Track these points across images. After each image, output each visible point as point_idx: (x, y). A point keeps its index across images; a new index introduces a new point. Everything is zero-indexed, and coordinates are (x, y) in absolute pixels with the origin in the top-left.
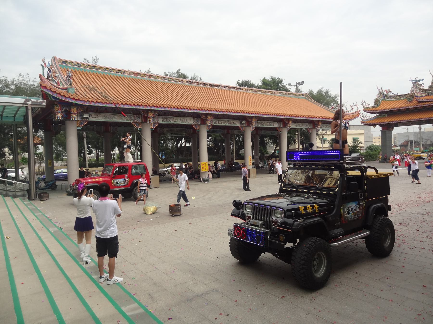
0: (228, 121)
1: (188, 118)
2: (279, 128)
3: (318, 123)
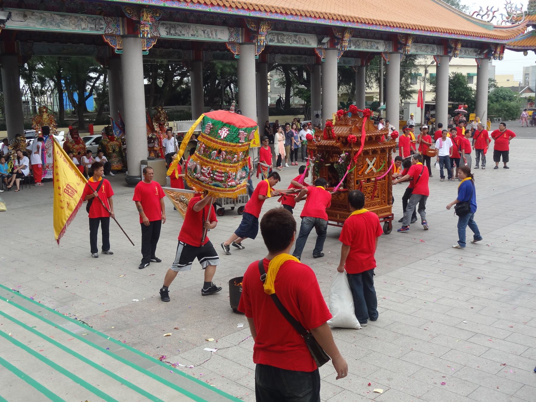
0: (296, 36)
1: (219, 28)
2: (385, 53)
3: (456, 45)
